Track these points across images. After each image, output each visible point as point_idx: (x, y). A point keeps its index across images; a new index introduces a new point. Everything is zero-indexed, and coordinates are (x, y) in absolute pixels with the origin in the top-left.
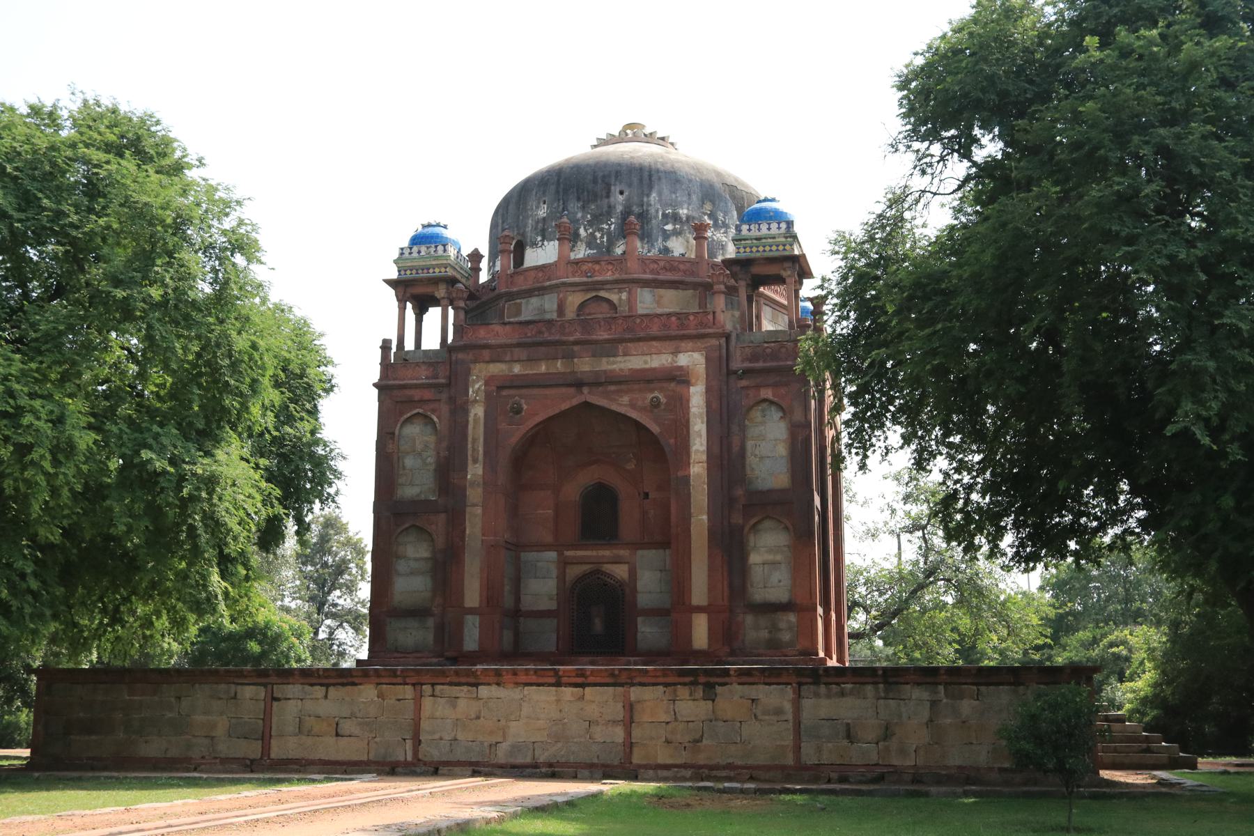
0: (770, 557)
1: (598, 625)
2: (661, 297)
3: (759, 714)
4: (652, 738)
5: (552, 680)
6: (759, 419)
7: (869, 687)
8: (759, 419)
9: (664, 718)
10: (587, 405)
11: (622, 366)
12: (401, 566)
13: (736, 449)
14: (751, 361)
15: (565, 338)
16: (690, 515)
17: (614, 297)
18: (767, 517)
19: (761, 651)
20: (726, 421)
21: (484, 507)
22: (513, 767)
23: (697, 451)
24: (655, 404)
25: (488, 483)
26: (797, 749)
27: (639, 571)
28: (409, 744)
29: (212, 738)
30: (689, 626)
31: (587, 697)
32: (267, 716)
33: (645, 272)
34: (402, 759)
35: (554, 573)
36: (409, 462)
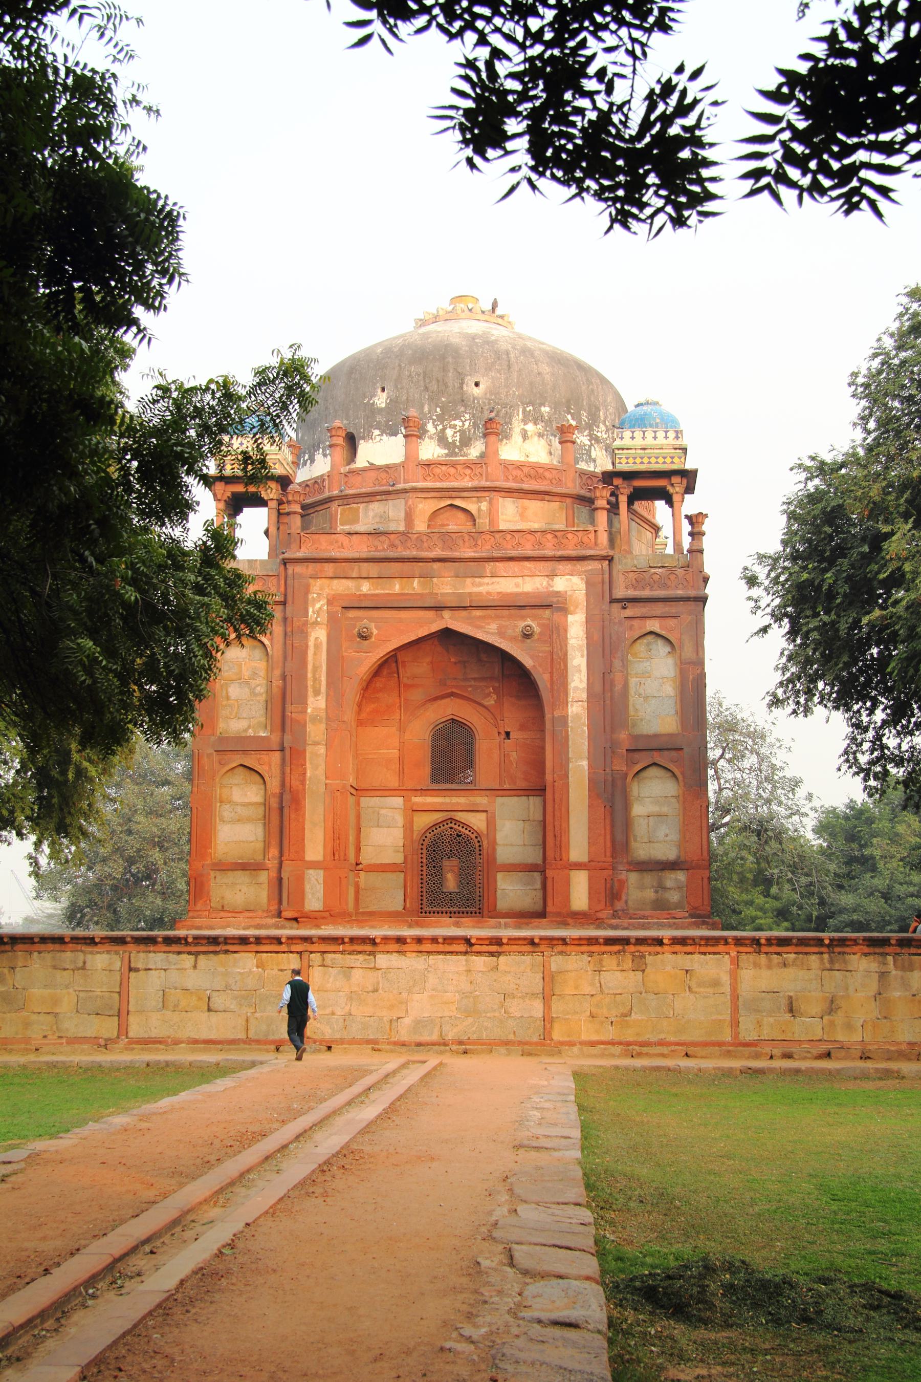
0: (655, 809)
1: (451, 882)
2: (525, 508)
3: (693, 984)
4: (576, 1013)
7: (814, 957)
9: (588, 990)
10: (447, 634)
11: (490, 588)
12: (226, 811)
13: (618, 687)
14: (635, 589)
16: (568, 760)
17: (472, 507)
18: (655, 764)
19: (647, 913)
21: (328, 746)
22: (419, 1044)
23: (576, 688)
24: (527, 635)
25: (331, 718)
26: (735, 1023)
27: (499, 822)
29: (56, 1015)
30: (567, 883)
31: (501, 967)
32: (123, 991)
33: (507, 480)
35: (400, 820)
36: (234, 691)
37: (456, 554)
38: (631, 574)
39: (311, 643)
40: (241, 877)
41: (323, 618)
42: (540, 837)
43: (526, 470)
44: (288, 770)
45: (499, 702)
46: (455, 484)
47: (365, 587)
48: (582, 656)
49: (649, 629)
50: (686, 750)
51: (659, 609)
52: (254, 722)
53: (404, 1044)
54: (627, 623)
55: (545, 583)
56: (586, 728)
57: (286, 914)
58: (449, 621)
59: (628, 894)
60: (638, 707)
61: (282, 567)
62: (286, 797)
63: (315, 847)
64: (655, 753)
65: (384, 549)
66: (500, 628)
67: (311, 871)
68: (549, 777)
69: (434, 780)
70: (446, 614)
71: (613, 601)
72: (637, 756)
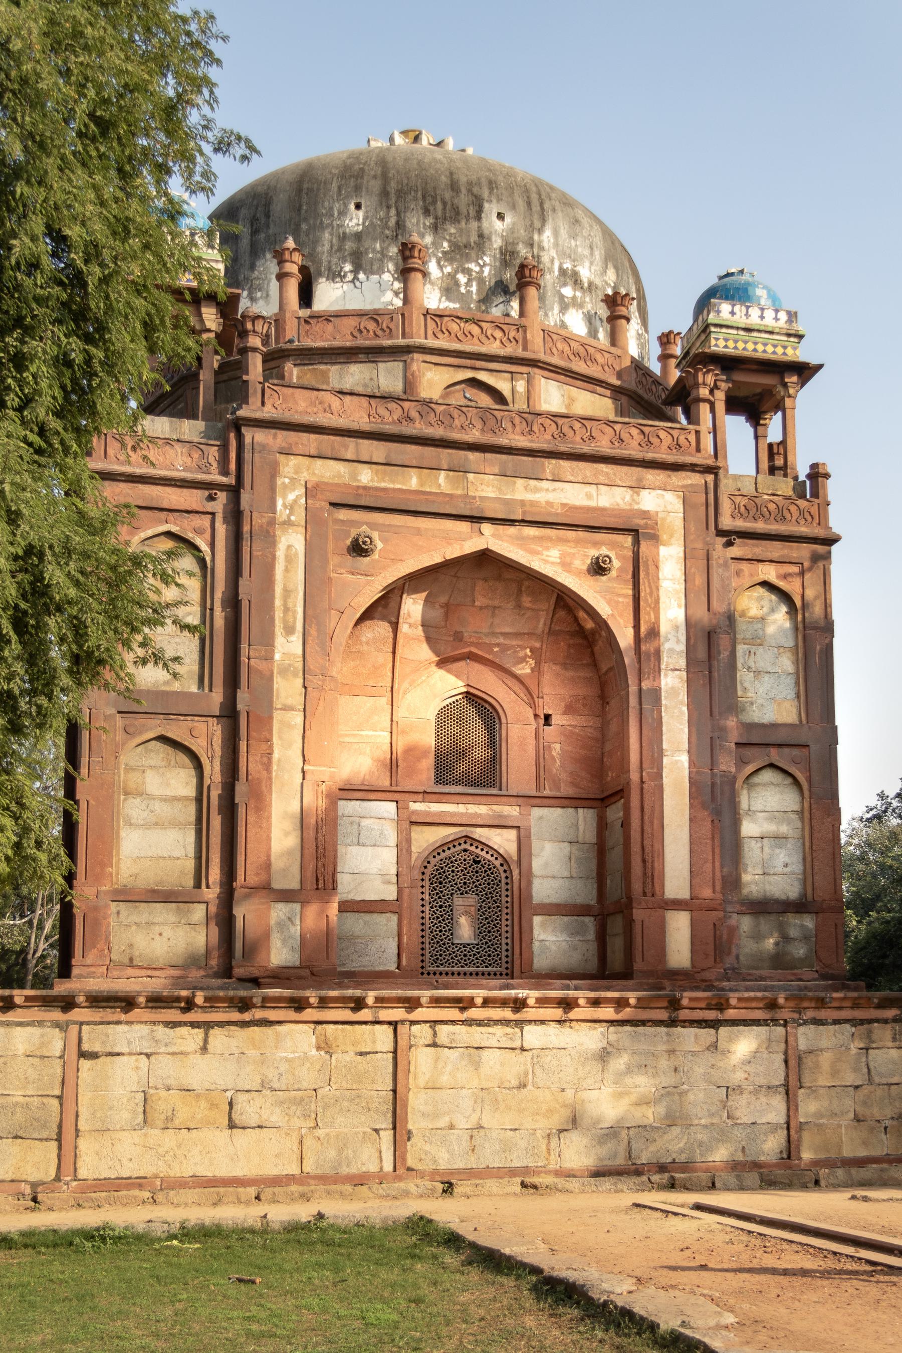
0: (770, 828)
1: (465, 930)
5: (663, 1015)
9: (850, 1078)
11: (551, 497)
12: (133, 809)
17: (503, 385)
18: (772, 766)
23: (671, 650)
27: (535, 844)
28: (387, 1136)
34: (373, 1168)
37: (504, 441)
38: (738, 499)
39: (280, 553)
40: (163, 913)
41: (299, 517)
42: (594, 866)
46: (483, 349)
47: (366, 476)
48: (679, 606)
49: (762, 577)
50: (813, 747)
51: (776, 549)
53: (570, 1175)
54: (734, 566)
55: (628, 498)
56: (685, 709)
57: (238, 971)
58: (490, 539)
60: (747, 685)
64: (773, 751)
65: (393, 422)
68: (634, 776)
70: (486, 528)
71: (720, 533)
72: (748, 752)
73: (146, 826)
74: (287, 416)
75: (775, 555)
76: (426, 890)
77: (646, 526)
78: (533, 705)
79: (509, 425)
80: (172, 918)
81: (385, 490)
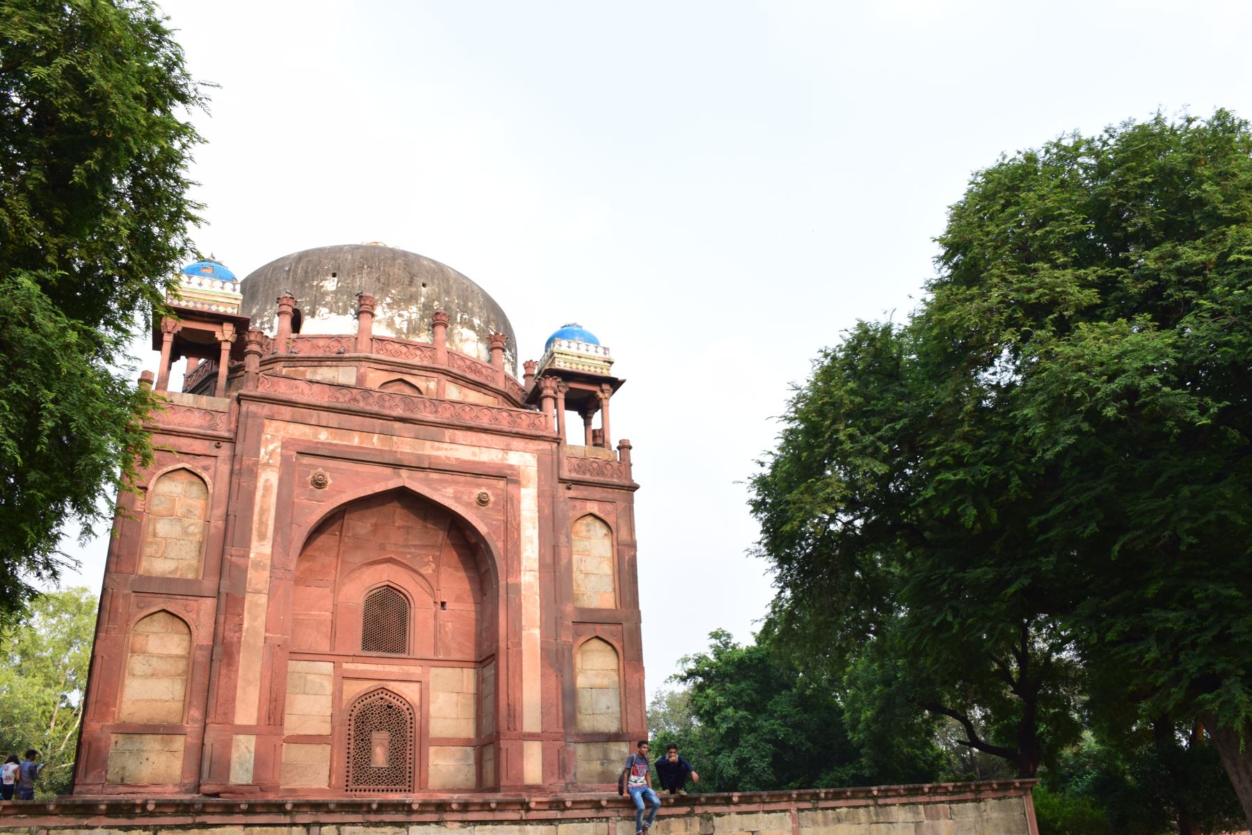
1: (380, 757)
6: (584, 534)
8: (584, 534)
12: (136, 664)
13: (564, 562)
15: (386, 412)
18: (597, 637)
19: (595, 785)
20: (554, 531)
23: (528, 558)
24: (482, 502)
27: (432, 695)
35: (329, 687)
37: (419, 416)
40: (151, 744)
43: (468, 363)
44: (222, 619)
45: (437, 571)
47: (323, 436)
51: (598, 493)
52: (183, 564)
54: (571, 503)
58: (406, 479)
59: (575, 766)
61: (235, 404)
62: (218, 650)
63: (247, 710)
64: (598, 627)
66: (456, 492)
67: (241, 737)
68: (502, 645)
69: (366, 646)
70: (404, 473)
71: (562, 481)
73: (145, 676)
74: (271, 393)
75: (597, 497)
76: (352, 728)
77: (512, 475)
78: (433, 595)
79: (422, 407)
80: (157, 746)
81: (336, 445)
